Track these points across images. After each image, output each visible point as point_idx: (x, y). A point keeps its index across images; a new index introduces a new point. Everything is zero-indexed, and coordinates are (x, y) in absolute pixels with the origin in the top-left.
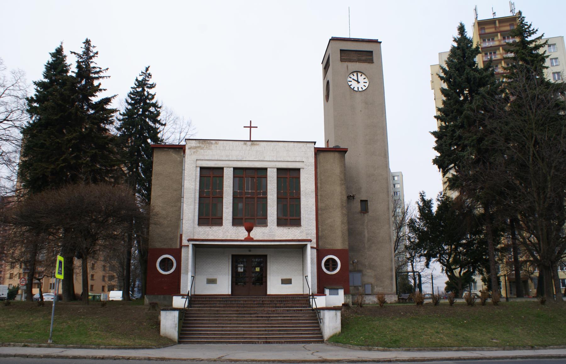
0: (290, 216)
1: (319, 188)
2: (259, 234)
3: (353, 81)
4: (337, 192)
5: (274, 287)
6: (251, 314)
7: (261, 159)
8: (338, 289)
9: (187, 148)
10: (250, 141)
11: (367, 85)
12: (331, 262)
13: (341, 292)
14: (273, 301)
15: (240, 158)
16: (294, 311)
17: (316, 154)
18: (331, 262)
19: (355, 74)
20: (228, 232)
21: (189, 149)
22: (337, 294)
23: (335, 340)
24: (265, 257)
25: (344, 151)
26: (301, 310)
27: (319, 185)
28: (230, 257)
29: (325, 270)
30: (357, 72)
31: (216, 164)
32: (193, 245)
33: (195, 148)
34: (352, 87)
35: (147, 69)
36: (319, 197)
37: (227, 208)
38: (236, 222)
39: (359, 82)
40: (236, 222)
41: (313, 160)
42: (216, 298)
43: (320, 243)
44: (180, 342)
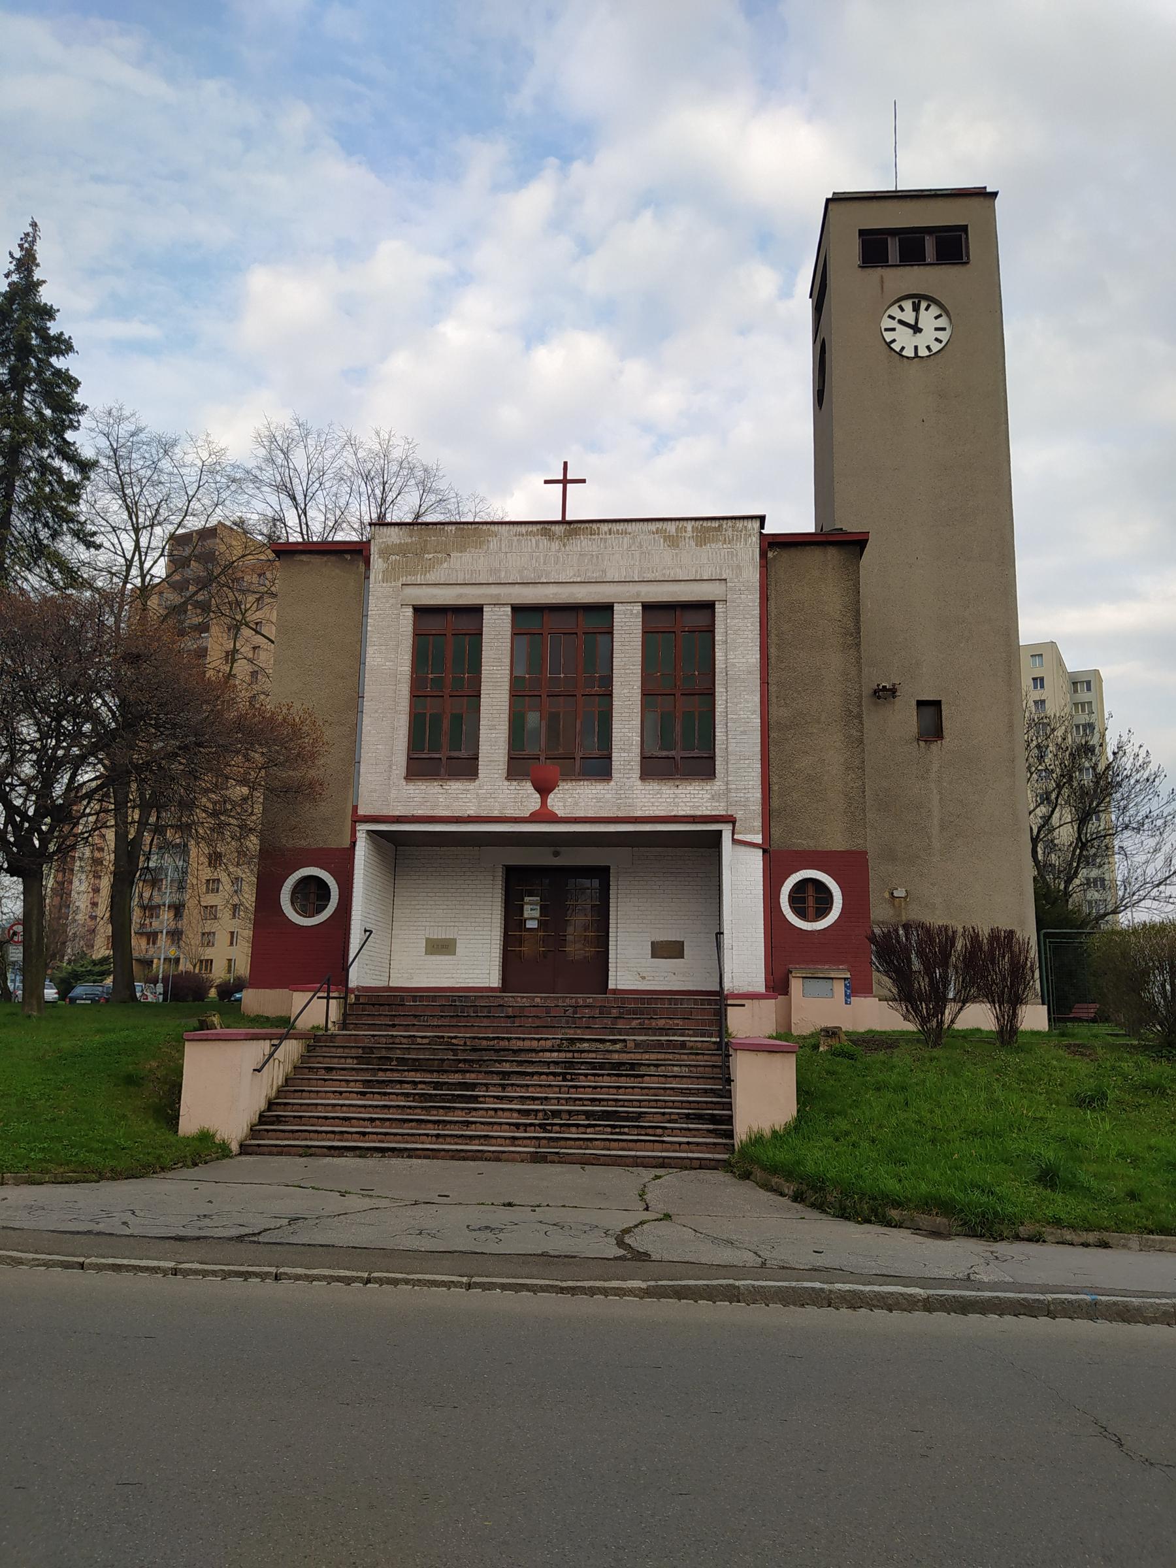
0: (684, 747)
1: (773, 661)
3: (899, 327)
5: (631, 967)
7: (596, 576)
9: (374, 549)
10: (564, 522)
11: (944, 336)
12: (811, 890)
15: (532, 577)
17: (763, 555)
18: (811, 890)
19: (908, 305)
25: (856, 544)
27: (773, 651)
30: (917, 300)
31: (460, 596)
32: (370, 833)
34: (896, 347)
39: (916, 329)
40: (517, 768)
43: (776, 832)
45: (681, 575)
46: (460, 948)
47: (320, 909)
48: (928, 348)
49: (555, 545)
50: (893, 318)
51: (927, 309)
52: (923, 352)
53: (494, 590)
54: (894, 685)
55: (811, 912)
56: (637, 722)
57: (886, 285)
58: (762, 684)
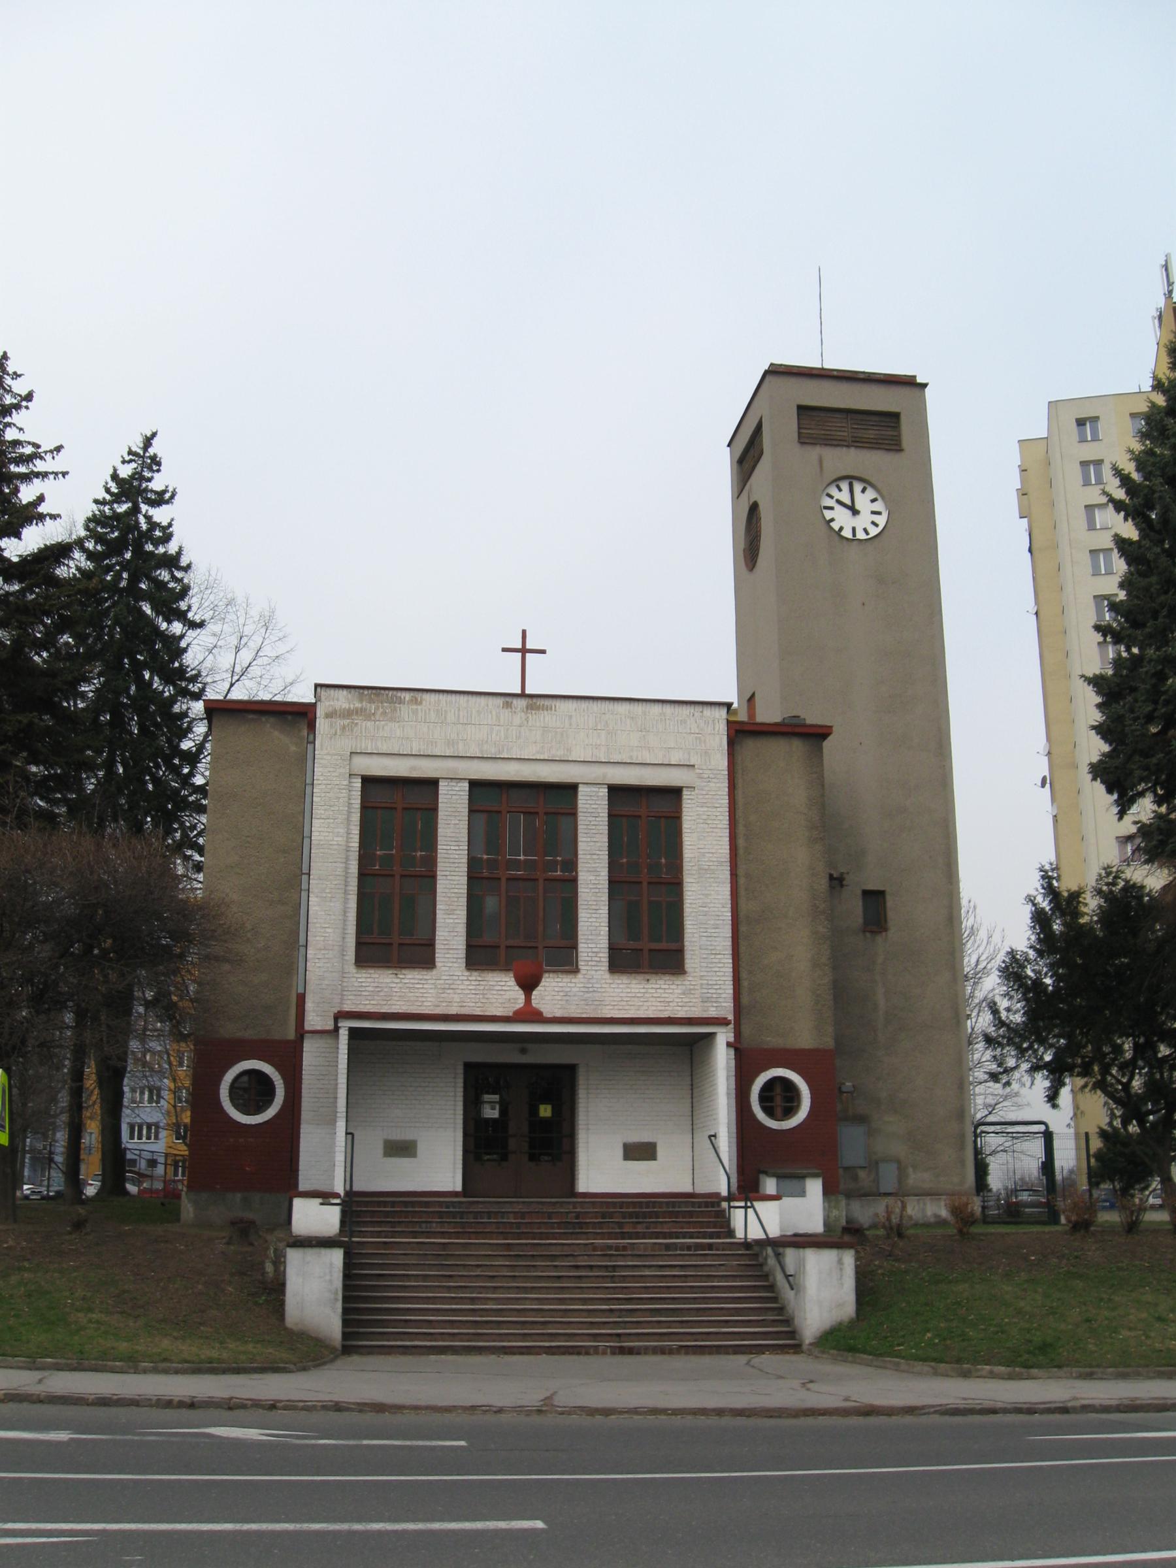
0: (649, 939)
1: (741, 852)
2: (556, 995)
3: (838, 507)
4: (797, 865)
5: (601, 1169)
6: (553, 1257)
7: (559, 754)
8: (803, 1177)
9: (320, 712)
10: (523, 695)
11: (882, 520)
12: (778, 1089)
13: (814, 1187)
14: (611, 1215)
15: (491, 751)
16: (689, 1247)
17: (731, 743)
18: (778, 1089)
19: (845, 486)
20: (451, 988)
21: (329, 715)
22: (802, 1193)
23: (840, 1341)
24: (571, 1070)
25: (817, 735)
26: (710, 1247)
27: (741, 842)
28: (460, 1070)
29: (761, 1115)
30: (851, 479)
31: (413, 768)
33: (348, 714)
34: (835, 526)
35: (148, 442)
36: (742, 881)
37: (450, 912)
38: (479, 956)
39: (855, 512)
40: (479, 956)
41: (721, 762)
42: (427, 1204)
43: (746, 1030)
44: (347, 1350)
45: (645, 757)
46: (421, 1148)
47: (258, 1110)
48: (865, 530)
49: (518, 719)
50: (832, 497)
51: (863, 491)
52: (861, 535)
53: (451, 764)
54: (842, 874)
55: (779, 1111)
56: (604, 910)
57: (825, 464)
58: (731, 875)
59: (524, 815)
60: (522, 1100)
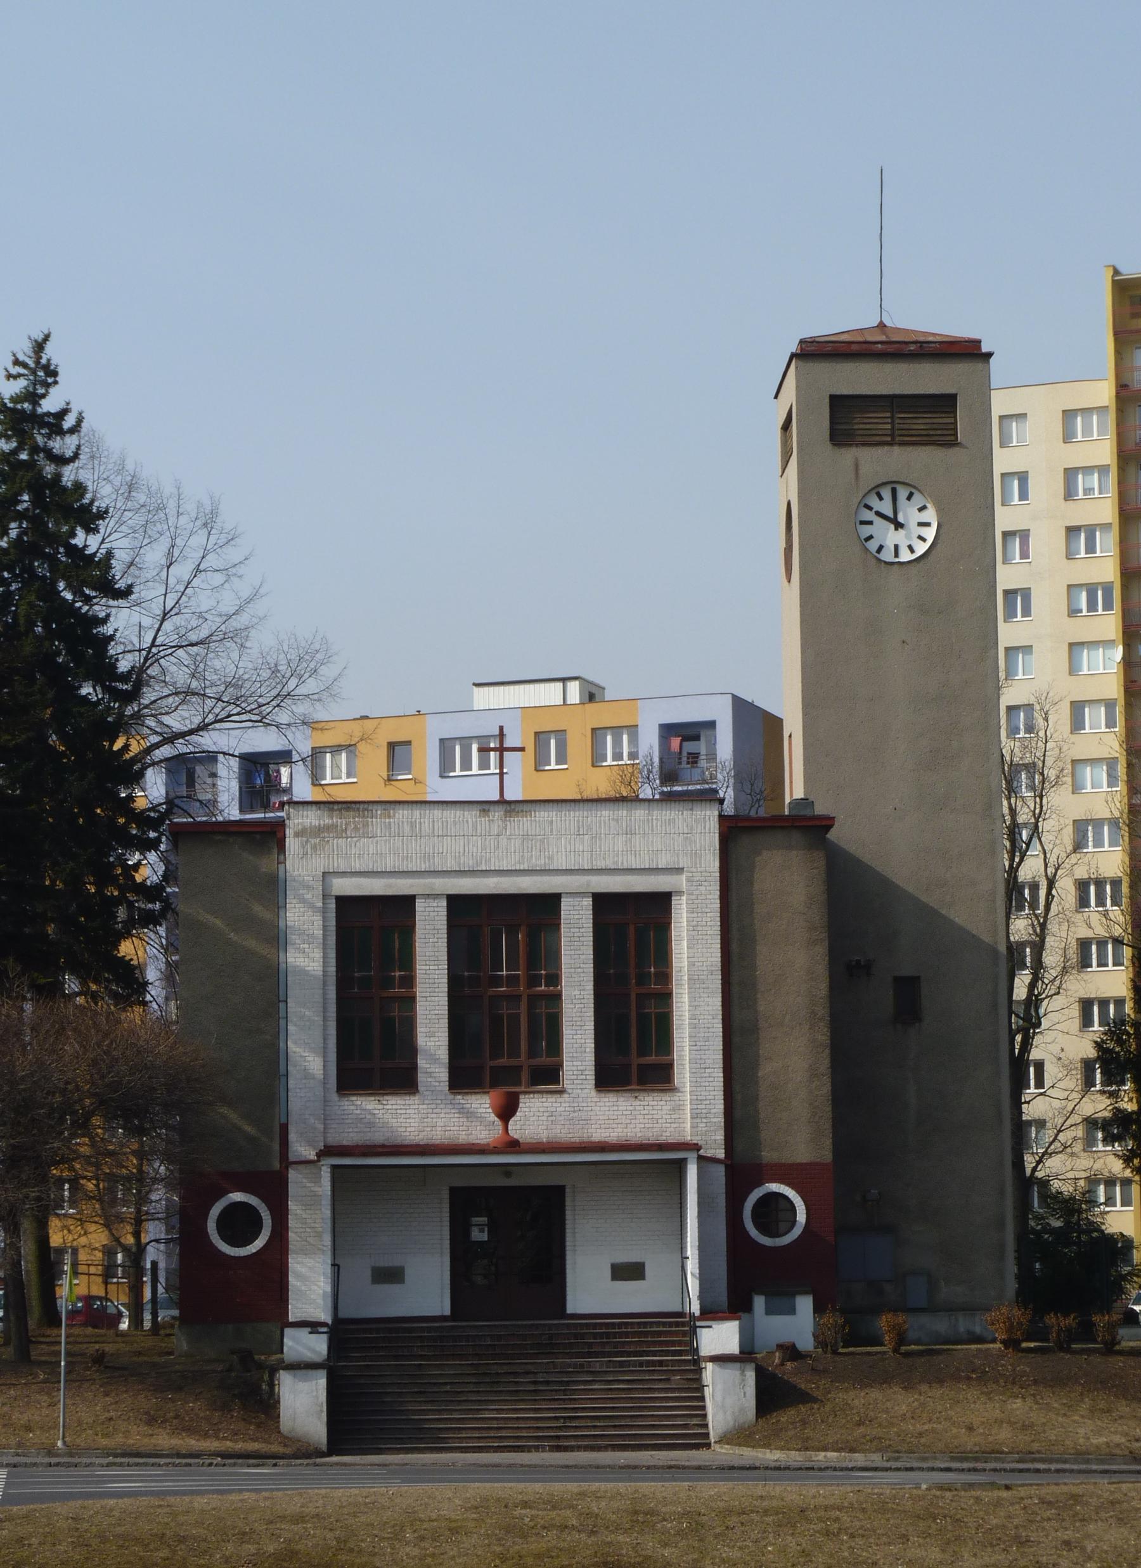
2: (539, 1117)
3: (878, 521)
4: (796, 969)
5: (590, 1290)
6: (516, 1374)
7: (539, 863)
8: (793, 1295)
11: (930, 534)
13: (805, 1304)
14: (583, 1336)
15: (468, 863)
16: (641, 1364)
19: (886, 493)
21: (297, 835)
22: (792, 1311)
23: (738, 1436)
24: (560, 1191)
26: (661, 1363)
27: (734, 947)
28: (446, 1195)
29: (753, 1232)
32: (334, 1168)
33: (318, 831)
35: (39, 347)
36: (735, 989)
37: (430, 1035)
38: (463, 1078)
39: (899, 526)
40: (463, 1078)
41: (713, 864)
42: (410, 1330)
44: (330, 1453)
46: (409, 1273)
50: (870, 508)
51: (909, 498)
59: (501, 930)
60: (513, 1224)
